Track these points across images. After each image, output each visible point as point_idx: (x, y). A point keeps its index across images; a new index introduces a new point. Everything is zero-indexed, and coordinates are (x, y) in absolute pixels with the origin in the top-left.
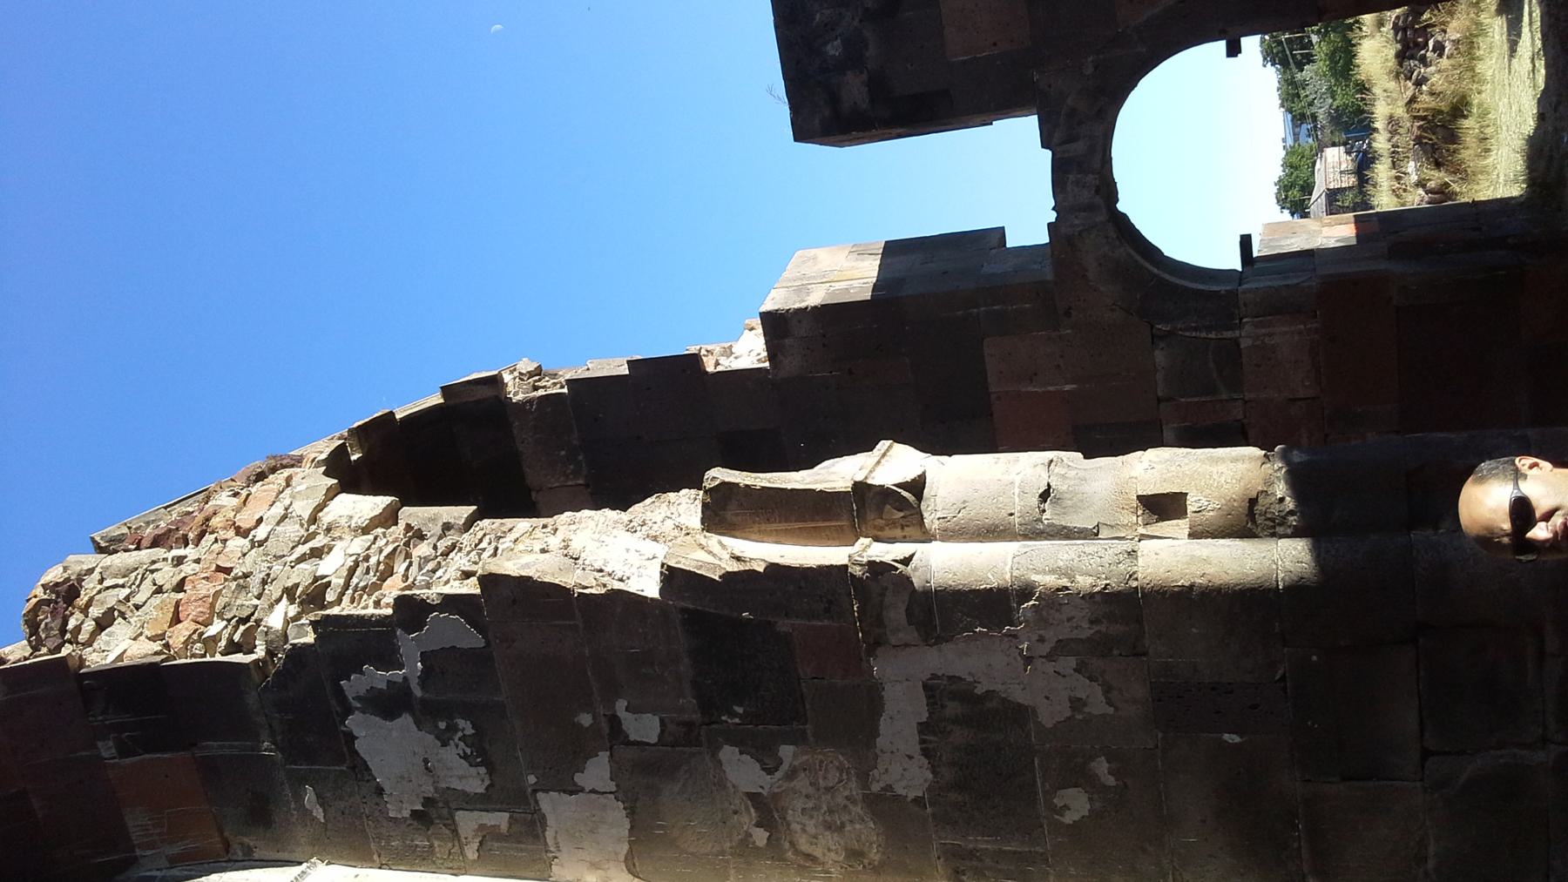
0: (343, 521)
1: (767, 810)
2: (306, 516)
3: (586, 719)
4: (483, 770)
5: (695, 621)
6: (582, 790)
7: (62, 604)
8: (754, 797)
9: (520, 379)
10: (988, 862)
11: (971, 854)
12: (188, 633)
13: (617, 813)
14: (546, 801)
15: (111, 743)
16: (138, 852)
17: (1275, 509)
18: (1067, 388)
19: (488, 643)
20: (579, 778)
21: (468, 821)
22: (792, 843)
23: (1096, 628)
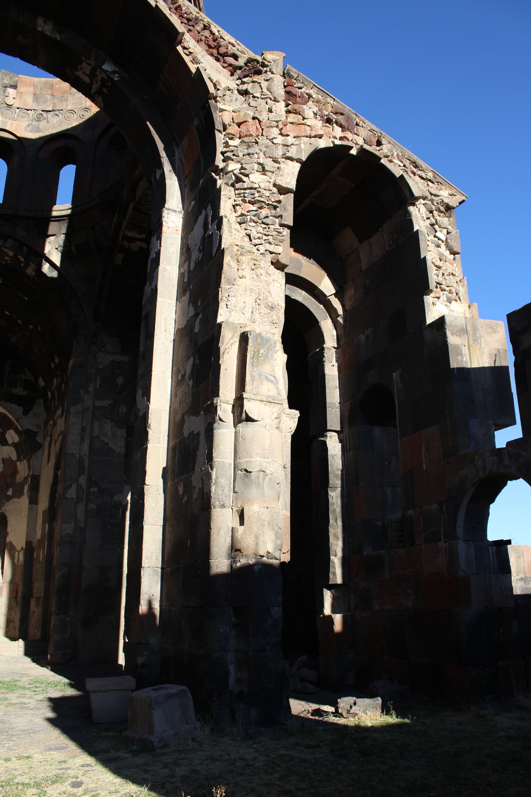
0: (281, 173)
2: (289, 154)
7: (253, 71)
9: (441, 202)
12: (232, 132)
15: (197, 122)
16: (180, 147)
17: (237, 559)
18: (424, 466)
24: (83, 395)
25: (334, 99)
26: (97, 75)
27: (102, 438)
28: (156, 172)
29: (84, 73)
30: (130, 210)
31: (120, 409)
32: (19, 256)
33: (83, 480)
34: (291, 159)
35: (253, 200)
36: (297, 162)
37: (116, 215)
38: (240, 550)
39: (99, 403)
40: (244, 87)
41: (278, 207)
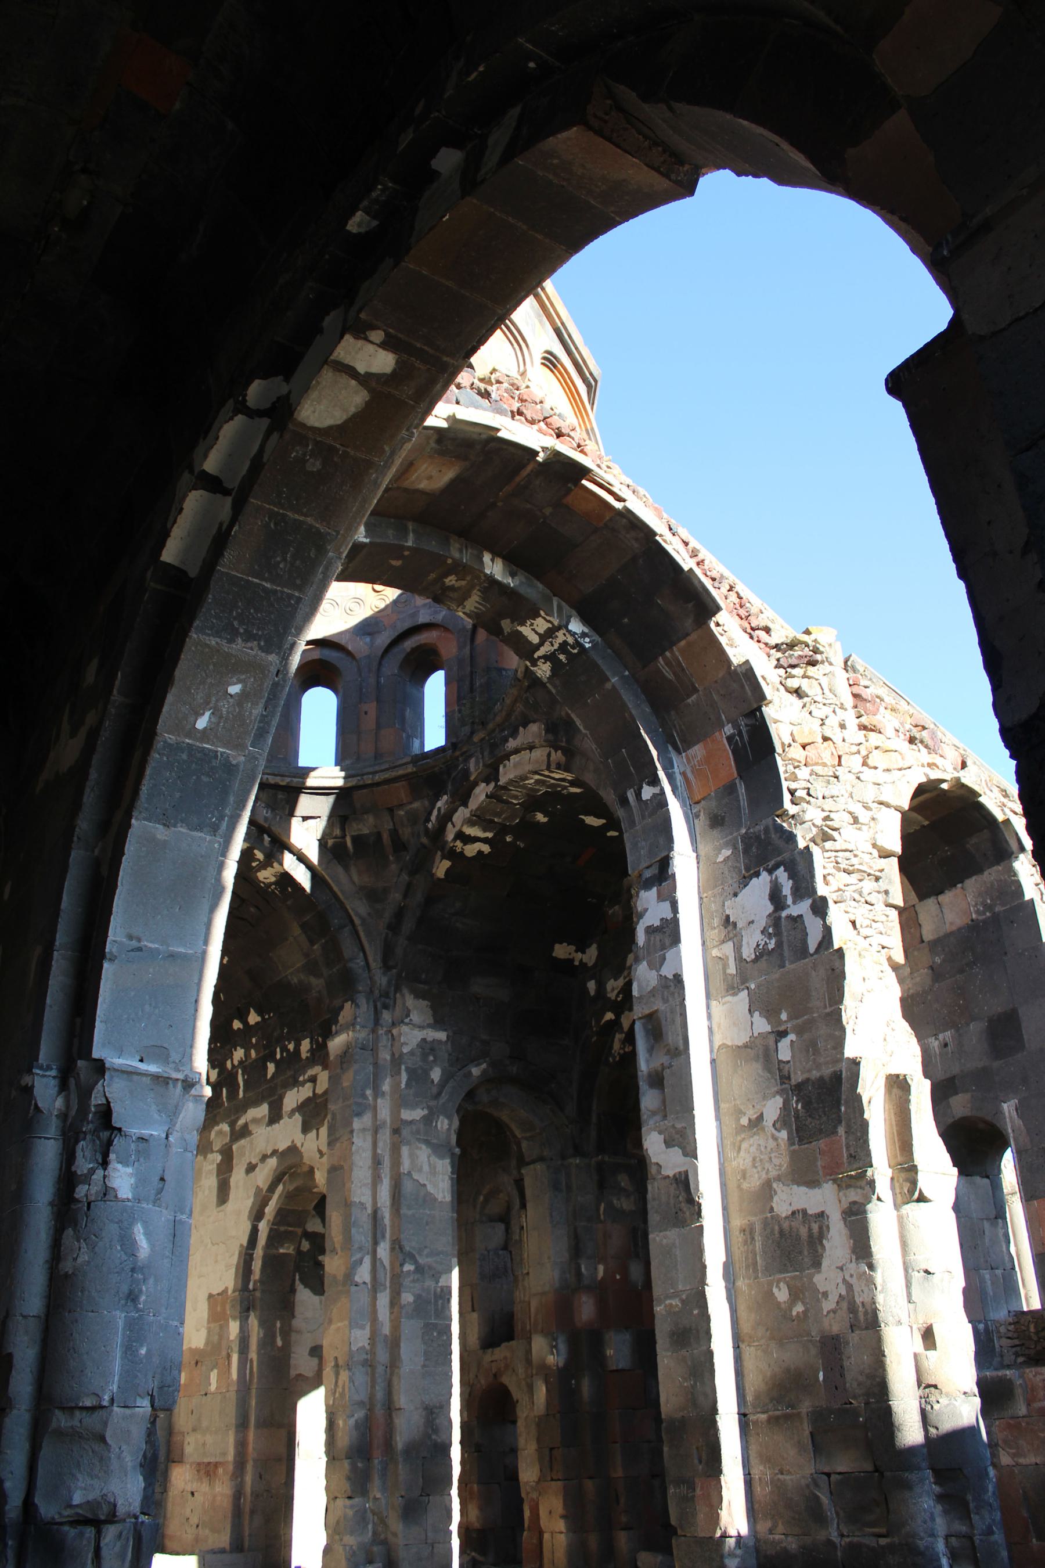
1: (757, 1122)
3: (784, 1016)
4: (753, 956)
5: (837, 1077)
6: (752, 1016)
8: (761, 1117)
10: (751, 1247)
11: (753, 1239)
13: (743, 1039)
14: (744, 994)
15: (732, 731)
16: (684, 754)
19: (812, 955)
20: (757, 1014)
21: (728, 948)
22: (744, 1139)
23: (860, 1305)
24: (370, 1098)
25: (909, 703)
26: (557, 637)
27: (415, 1176)
28: (641, 787)
29: (533, 630)
30: (481, 793)
31: (439, 1124)
32: (256, 852)
33: (383, 1251)
34: (888, 805)
35: (851, 868)
36: (896, 810)
37: (445, 797)
38: (935, 1387)
39: (407, 1115)
40: (793, 683)
41: (881, 878)
